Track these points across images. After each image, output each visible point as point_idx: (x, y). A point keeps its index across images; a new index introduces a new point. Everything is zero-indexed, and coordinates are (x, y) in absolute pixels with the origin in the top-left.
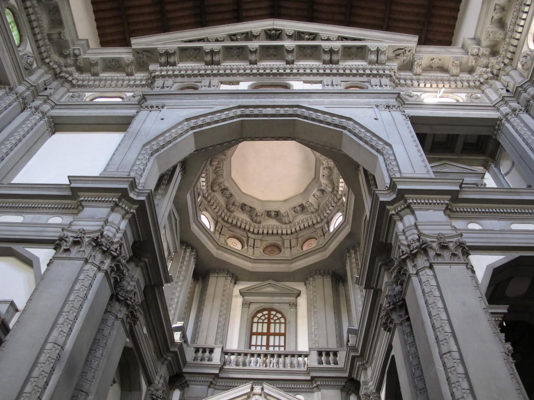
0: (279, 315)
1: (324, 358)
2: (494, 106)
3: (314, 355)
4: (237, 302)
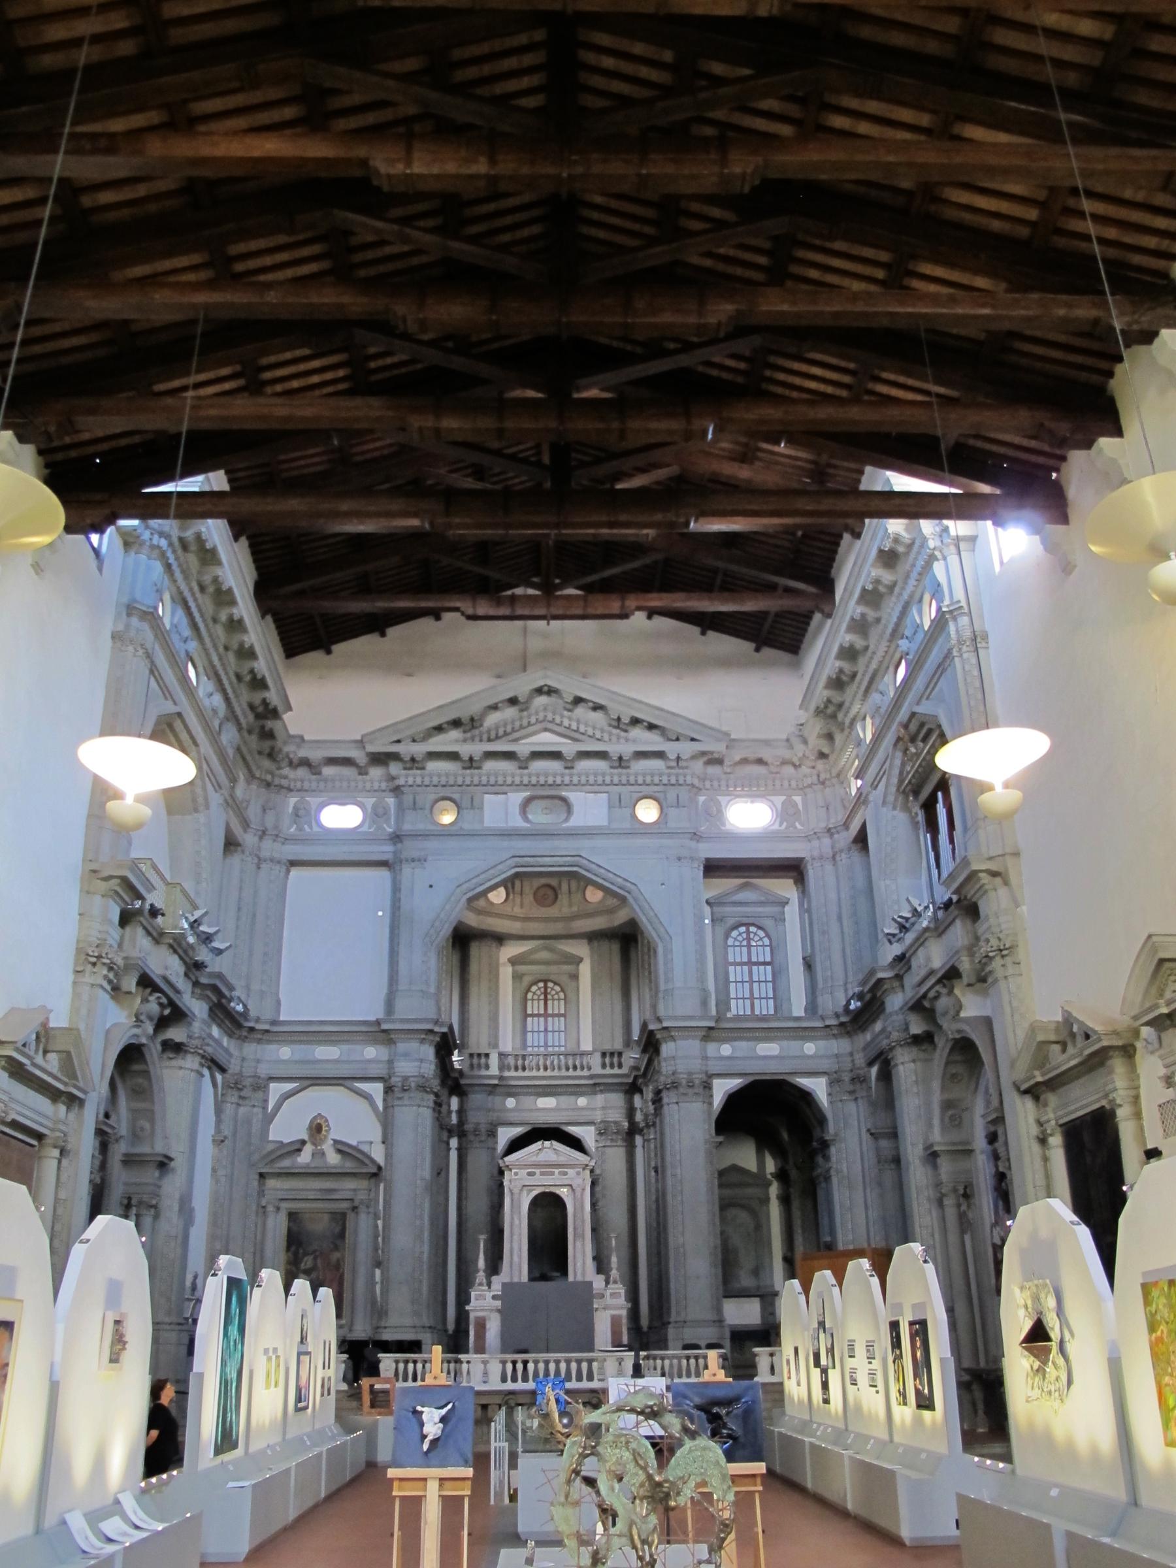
0: (558, 988)
1: (607, 1060)
3: (596, 1061)
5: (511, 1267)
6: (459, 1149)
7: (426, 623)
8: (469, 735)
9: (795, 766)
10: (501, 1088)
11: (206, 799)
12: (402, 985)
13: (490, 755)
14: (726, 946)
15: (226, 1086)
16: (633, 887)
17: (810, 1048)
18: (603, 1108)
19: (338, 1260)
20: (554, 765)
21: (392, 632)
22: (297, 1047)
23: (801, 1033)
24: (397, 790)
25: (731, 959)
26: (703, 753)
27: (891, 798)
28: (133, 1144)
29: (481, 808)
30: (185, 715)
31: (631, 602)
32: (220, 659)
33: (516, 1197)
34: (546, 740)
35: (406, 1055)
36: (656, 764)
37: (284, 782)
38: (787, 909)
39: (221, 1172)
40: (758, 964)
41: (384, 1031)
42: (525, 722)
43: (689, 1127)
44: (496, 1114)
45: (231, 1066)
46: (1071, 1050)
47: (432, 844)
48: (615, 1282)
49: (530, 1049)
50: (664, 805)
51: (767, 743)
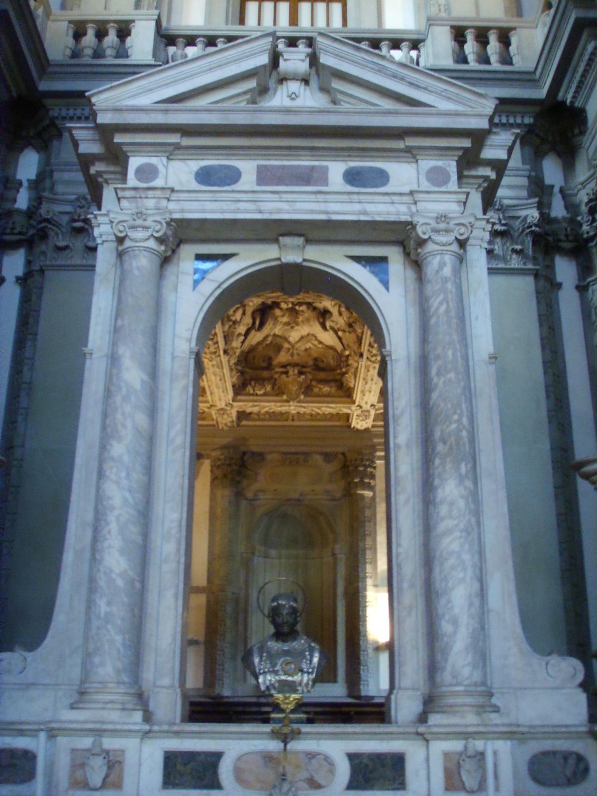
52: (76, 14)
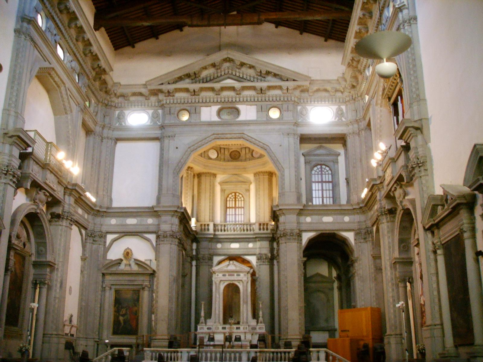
0: (240, 196)
2: (347, 124)
4: (218, 188)
5: (215, 316)
6: (196, 266)
7: (176, 33)
8: (194, 81)
9: (342, 93)
10: (215, 239)
11: (70, 107)
12: (164, 192)
13: (202, 89)
14: (311, 174)
15: (87, 235)
16: (267, 147)
17: (347, 219)
18: (260, 248)
19: (136, 311)
20: (231, 94)
21: (162, 37)
22: (118, 219)
23: (343, 212)
24: (162, 106)
25: (313, 180)
26: (299, 86)
27: (379, 102)
28: (38, 258)
29: (200, 113)
30: (55, 68)
31: (263, 17)
32: (75, 45)
33: (218, 285)
34: (229, 82)
35: (165, 222)
36: (278, 92)
37: (113, 104)
38: (339, 158)
39: (85, 272)
40: (326, 182)
41: (155, 211)
42: (219, 75)
43: (291, 254)
44: (212, 250)
45: (90, 227)
46: (446, 207)
47: (176, 130)
48: (261, 323)
49: (228, 222)
50: (282, 110)
51: (329, 81)
52: (201, 223)
